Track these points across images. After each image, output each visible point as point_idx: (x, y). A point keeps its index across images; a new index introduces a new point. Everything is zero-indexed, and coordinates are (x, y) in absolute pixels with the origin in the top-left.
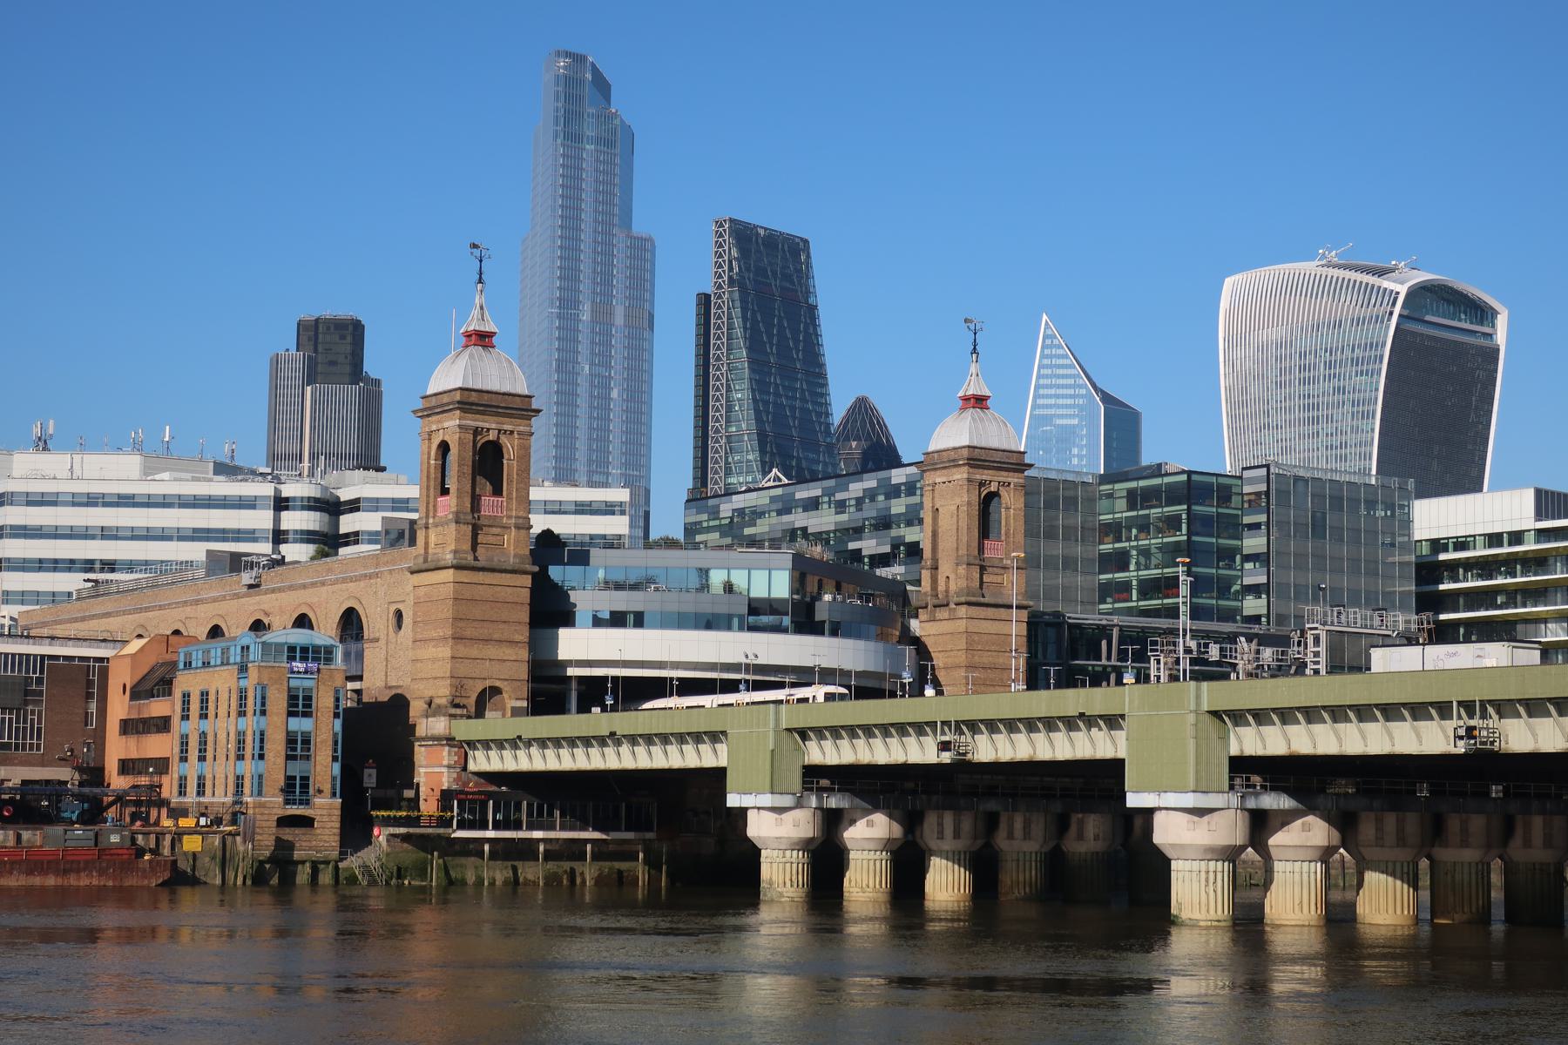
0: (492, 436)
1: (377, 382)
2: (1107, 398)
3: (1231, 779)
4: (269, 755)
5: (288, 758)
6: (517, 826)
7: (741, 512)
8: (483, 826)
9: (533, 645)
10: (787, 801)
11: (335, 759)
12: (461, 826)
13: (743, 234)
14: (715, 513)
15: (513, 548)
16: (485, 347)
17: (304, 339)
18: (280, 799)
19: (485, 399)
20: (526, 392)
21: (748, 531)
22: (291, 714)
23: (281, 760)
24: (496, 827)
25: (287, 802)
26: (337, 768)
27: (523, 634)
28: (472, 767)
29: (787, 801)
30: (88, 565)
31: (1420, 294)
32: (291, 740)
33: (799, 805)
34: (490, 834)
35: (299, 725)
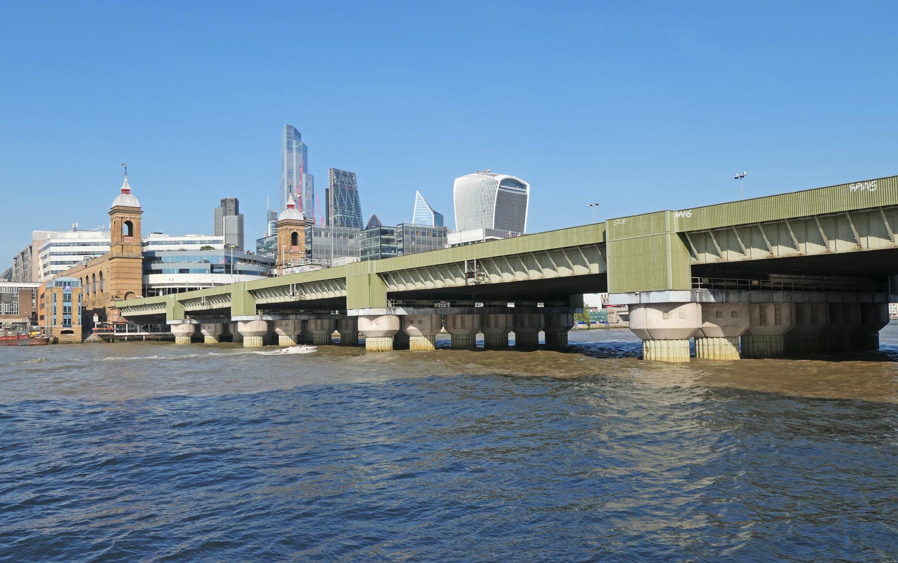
0: (128, 219)
1: (243, 215)
2: (435, 213)
3: (257, 311)
4: (57, 313)
5: (64, 314)
6: (136, 331)
7: (268, 242)
8: (125, 331)
9: (143, 279)
10: (179, 322)
11: (79, 314)
12: (117, 332)
13: (337, 173)
14: (263, 243)
15: (136, 251)
16: (127, 193)
17: (223, 204)
18: (62, 326)
19: (125, 209)
20: (138, 205)
21: (270, 248)
22: (64, 301)
23: (62, 315)
24: (129, 331)
25: (64, 327)
26: (80, 316)
27: (140, 276)
28: (122, 315)
29: (179, 322)
30: (69, 263)
31: (504, 182)
32: (65, 308)
33: (183, 323)
34: (127, 334)
35: (67, 304)
